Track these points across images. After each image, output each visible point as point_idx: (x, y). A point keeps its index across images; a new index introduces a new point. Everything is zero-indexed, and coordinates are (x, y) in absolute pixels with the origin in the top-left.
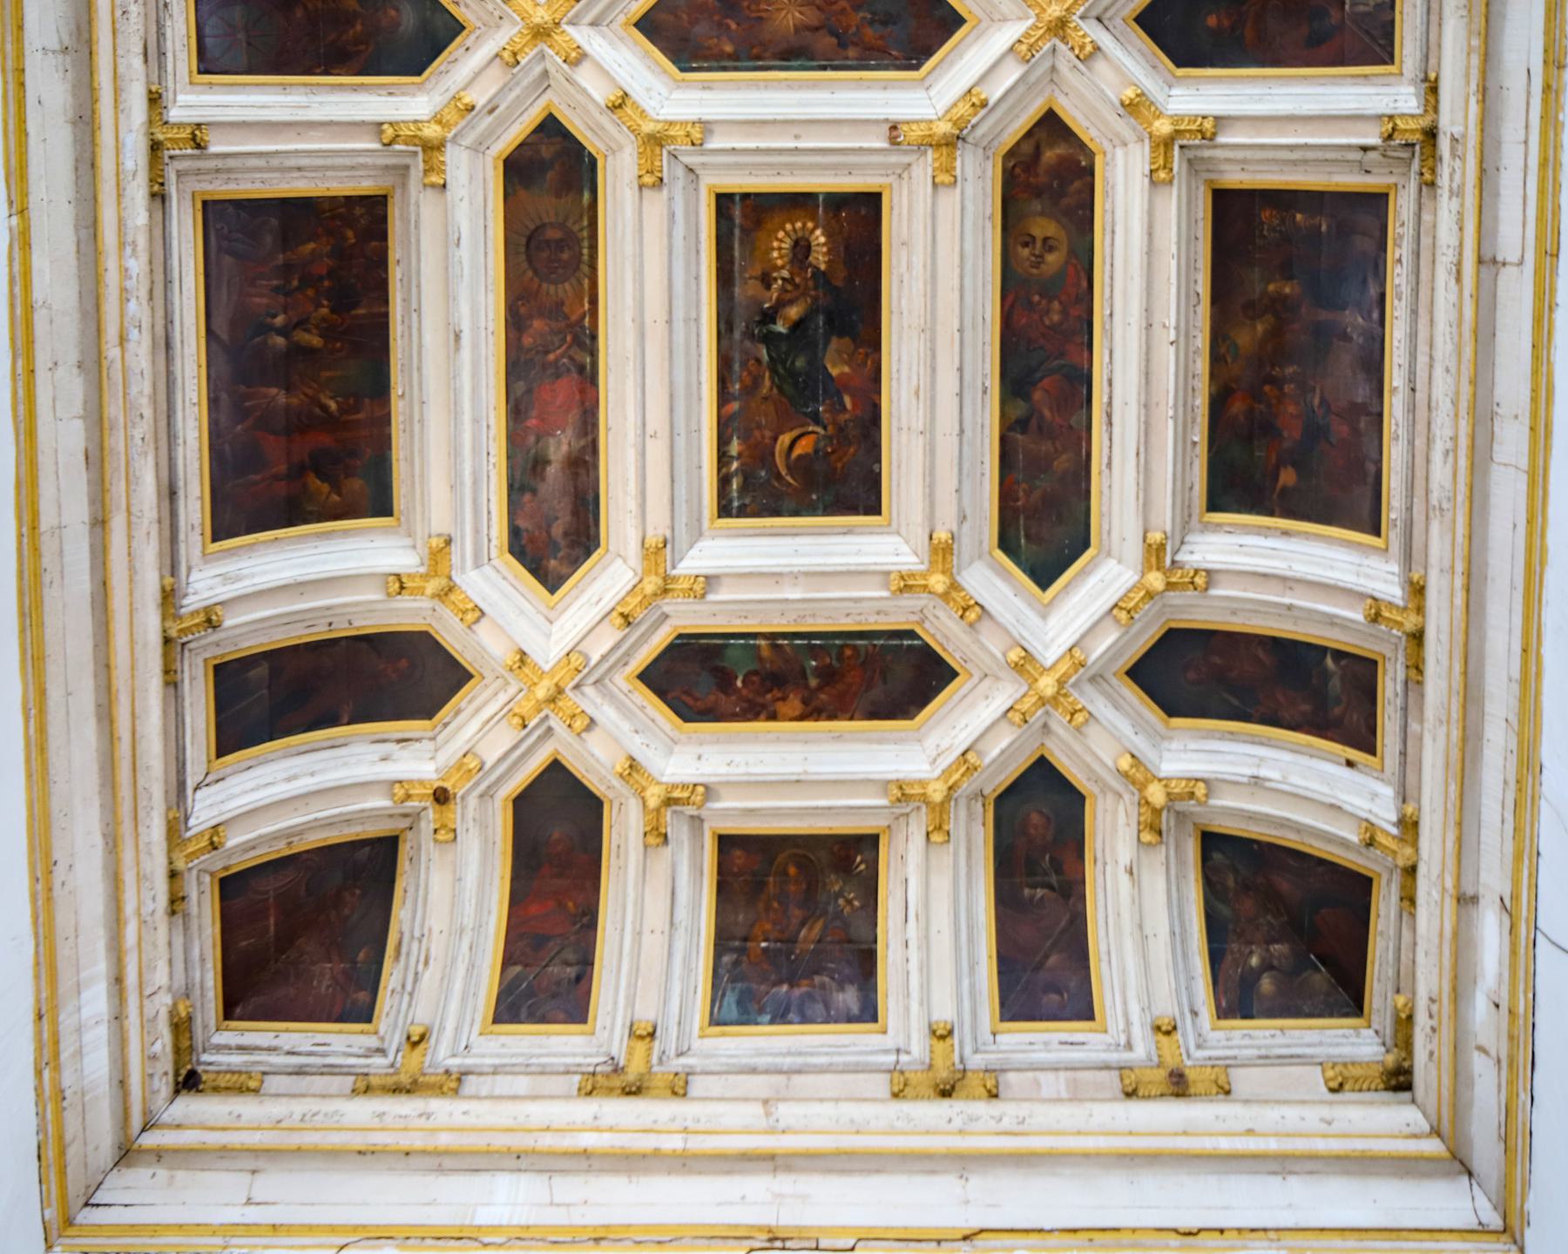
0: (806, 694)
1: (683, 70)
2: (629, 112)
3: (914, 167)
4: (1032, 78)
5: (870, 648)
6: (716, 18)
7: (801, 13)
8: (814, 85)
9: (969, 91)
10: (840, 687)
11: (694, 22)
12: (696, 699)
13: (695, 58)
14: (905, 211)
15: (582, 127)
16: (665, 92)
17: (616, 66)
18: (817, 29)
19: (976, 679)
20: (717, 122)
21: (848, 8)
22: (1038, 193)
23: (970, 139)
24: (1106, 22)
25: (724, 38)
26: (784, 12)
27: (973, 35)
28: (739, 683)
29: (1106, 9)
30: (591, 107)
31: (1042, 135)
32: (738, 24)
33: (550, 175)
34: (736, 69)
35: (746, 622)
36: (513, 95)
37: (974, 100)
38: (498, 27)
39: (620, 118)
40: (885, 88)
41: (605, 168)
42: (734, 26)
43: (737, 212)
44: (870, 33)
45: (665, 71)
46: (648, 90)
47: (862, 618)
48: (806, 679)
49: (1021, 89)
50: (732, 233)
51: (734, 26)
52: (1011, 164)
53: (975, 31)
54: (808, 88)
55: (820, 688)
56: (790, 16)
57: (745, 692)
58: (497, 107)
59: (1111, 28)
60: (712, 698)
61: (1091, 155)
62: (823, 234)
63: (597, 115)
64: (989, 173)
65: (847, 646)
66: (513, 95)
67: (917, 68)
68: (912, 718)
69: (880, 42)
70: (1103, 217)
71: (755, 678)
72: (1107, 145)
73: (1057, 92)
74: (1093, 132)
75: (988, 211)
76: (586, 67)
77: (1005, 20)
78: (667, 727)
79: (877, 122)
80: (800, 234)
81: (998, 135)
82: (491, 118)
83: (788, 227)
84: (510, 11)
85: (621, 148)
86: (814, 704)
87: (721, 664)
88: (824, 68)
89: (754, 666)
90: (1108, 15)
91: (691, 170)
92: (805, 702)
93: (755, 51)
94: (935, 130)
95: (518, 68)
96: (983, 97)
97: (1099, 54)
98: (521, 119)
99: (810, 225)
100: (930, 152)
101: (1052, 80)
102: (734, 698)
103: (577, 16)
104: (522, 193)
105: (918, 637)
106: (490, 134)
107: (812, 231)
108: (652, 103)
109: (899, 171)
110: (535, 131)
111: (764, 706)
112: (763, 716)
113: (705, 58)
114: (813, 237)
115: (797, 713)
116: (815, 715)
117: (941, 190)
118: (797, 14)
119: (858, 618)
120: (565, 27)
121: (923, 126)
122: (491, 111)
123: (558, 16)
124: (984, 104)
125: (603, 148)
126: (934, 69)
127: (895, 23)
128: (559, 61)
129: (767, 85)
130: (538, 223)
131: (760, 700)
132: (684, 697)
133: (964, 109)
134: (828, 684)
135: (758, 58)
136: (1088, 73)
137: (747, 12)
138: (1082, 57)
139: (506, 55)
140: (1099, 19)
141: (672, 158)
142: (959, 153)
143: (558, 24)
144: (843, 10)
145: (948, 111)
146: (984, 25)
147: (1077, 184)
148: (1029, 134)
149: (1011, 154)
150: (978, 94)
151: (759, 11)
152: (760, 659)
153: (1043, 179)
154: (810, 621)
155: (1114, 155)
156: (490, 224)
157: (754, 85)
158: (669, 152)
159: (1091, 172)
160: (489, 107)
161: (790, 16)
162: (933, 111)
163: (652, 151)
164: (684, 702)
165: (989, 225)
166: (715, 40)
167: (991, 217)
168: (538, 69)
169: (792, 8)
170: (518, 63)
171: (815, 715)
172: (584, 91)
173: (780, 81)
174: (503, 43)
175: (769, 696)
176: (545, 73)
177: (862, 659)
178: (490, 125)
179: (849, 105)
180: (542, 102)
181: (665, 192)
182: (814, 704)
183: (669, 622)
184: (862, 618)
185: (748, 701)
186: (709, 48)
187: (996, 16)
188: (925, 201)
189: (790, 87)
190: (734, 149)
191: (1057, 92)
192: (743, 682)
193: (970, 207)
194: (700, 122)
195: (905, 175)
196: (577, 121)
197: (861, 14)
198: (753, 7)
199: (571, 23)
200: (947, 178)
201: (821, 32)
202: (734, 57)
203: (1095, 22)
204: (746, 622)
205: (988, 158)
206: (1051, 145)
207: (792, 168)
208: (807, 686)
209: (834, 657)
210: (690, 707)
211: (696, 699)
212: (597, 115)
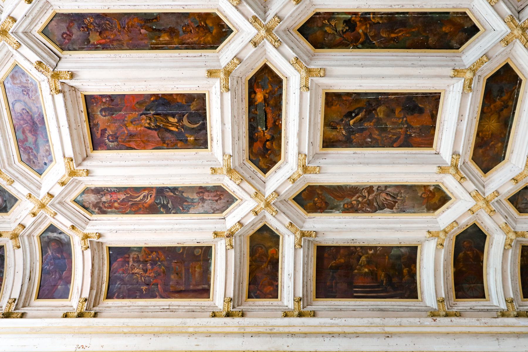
120: (486, 197)
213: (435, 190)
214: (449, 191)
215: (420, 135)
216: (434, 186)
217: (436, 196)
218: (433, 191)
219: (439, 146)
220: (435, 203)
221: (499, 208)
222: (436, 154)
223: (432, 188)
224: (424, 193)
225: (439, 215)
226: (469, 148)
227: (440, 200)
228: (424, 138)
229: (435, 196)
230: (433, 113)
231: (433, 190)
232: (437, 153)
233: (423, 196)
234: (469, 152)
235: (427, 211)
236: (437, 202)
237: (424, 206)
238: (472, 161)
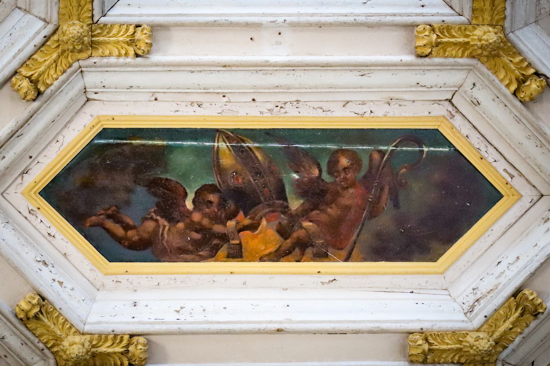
0: (284, 219)
5: (376, 156)
10: (333, 211)
12: (127, 227)
19: (525, 203)
28: (189, 204)
35: (200, 112)
47: (366, 108)
48: (285, 199)
55: (305, 213)
57: (196, 217)
60: (150, 225)
65: (343, 152)
68: (434, 260)
71: (213, 197)
78: (86, 266)
86: (298, 233)
87: (164, 176)
89: (212, 180)
92: (283, 232)
102: (181, 225)
105: (443, 141)
111: (224, 238)
112: (223, 252)
115: (272, 249)
116: (297, 251)
119: (360, 109)
131: (218, 228)
132: (110, 224)
134: (315, 207)
152: (220, 170)
154: (291, 111)
164: (108, 231)
171: (297, 251)
175: (231, 224)
177: (362, 173)
182: (298, 233)
183: (93, 109)
184: (366, 108)
185: (200, 229)
192: (194, 202)
204: (200, 112)
208: (285, 209)
209: (324, 168)
210: (119, 240)
211: (127, 227)
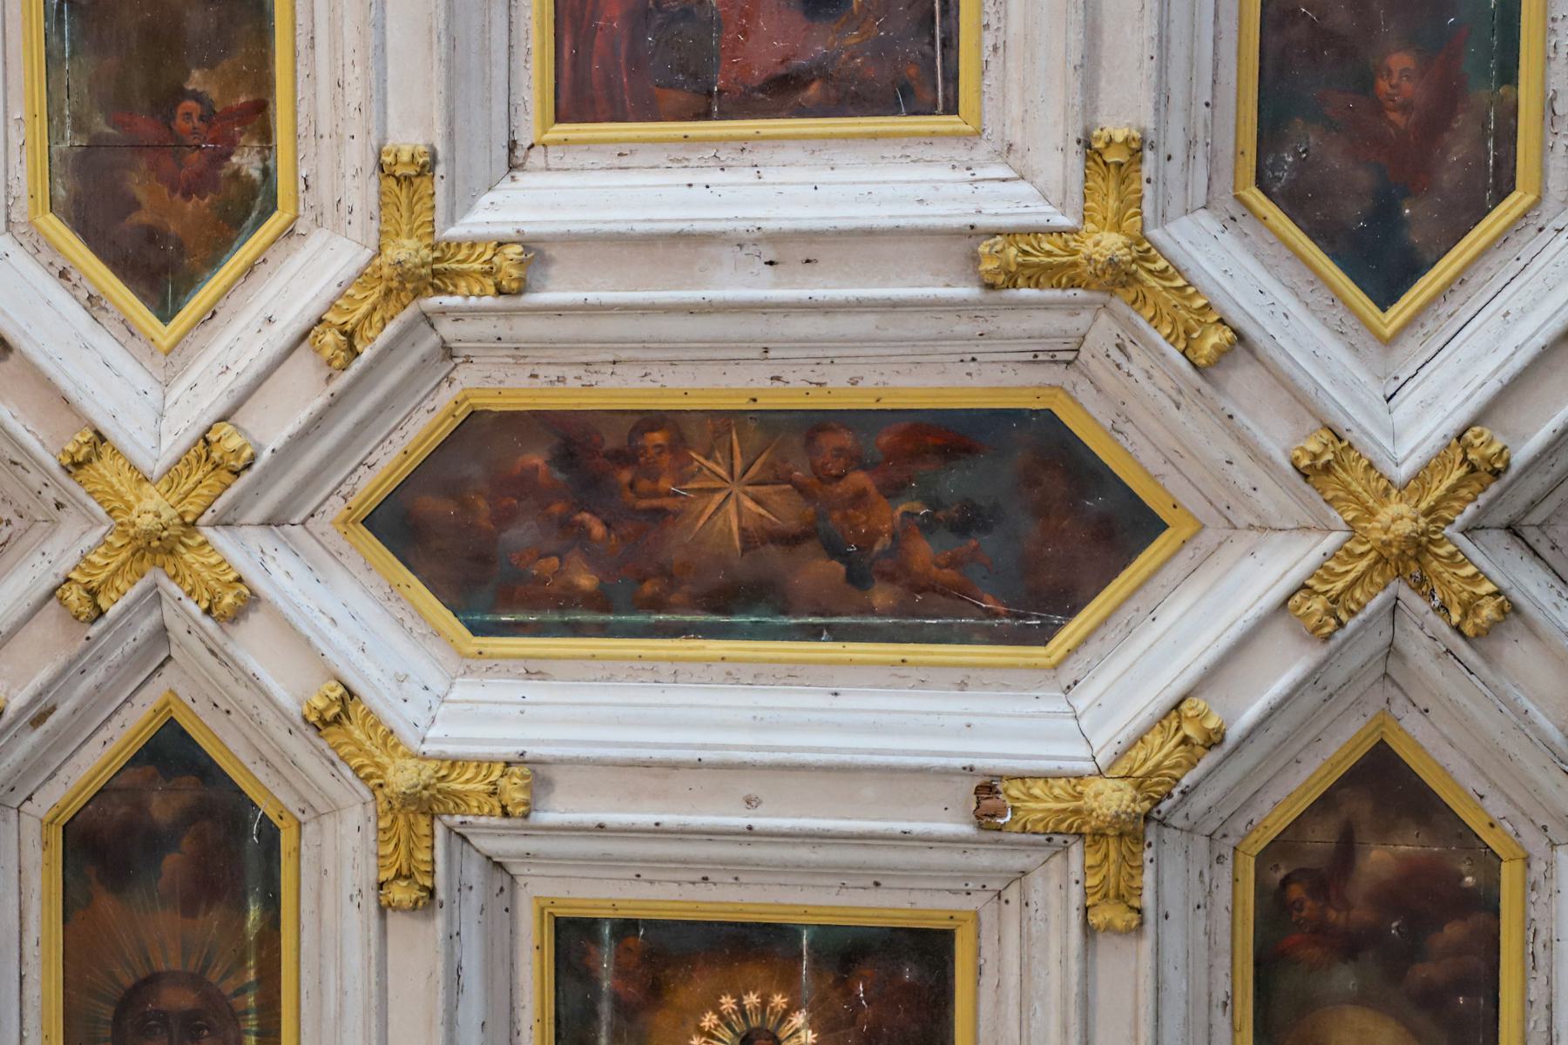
1: (477, 630)
2: (358, 734)
3: (1036, 880)
4: (1336, 676)
6: (556, 509)
7: (758, 502)
8: (791, 674)
9: (1177, 707)
11: (504, 518)
13: (507, 599)
14: (1012, 980)
15: (246, 757)
16: (438, 685)
17: (324, 623)
18: (790, 540)
20: (561, 761)
21: (873, 490)
22: (1350, 947)
23: (1176, 819)
24: (1531, 535)
25: (575, 558)
26: (719, 497)
27: (1182, 562)
29: (1533, 505)
30: (268, 716)
31: (1360, 807)
32: (608, 525)
33: (172, 862)
34: (604, 631)
36: (89, 681)
37: (1188, 729)
38: (53, 523)
39: (335, 748)
40: (963, 686)
41: (298, 850)
42: (598, 530)
43: (605, 962)
44: (924, 553)
45: (438, 633)
46: (401, 679)
49: (1310, 699)
50: (595, 1015)
51: (598, 530)
52: (1280, 875)
53: (1188, 552)
54: (776, 680)
56: (731, 507)
58: (54, 709)
59: (1543, 548)
61: (1490, 862)
62: (811, 1024)
63: (282, 735)
64: (1224, 895)
66: (89, 681)
67: (1042, 637)
69: (948, 575)
70: (1524, 1019)
72: (1533, 841)
73: (1399, 702)
74: (1495, 806)
75: (1222, 988)
76: (255, 627)
77: (1265, 528)
79: (945, 773)
80: (755, 1021)
81: (1246, 805)
82: (36, 736)
83: (728, 1003)
84: (81, 493)
85: (336, 809)
88: (813, 634)
90: (1537, 517)
91: (499, 866)
93: (649, 588)
94: (1089, 802)
95: (101, 624)
96: (1212, 724)
97: (1515, 621)
98: (104, 734)
99: (779, 1001)
100: (1076, 850)
101: (1386, 675)
103: (234, 505)
104: (106, 904)
106: (38, 767)
107: (785, 1016)
108: (412, 712)
109: (998, 886)
110: (134, 761)
113: (533, 604)
114: (785, 1031)
117: (1104, 943)
118: (749, 504)
121: (1059, 787)
122: (38, 721)
123: (192, 509)
124: (1213, 740)
125: (293, 806)
126: (1084, 641)
127: (986, 528)
128: (197, 611)
129: (678, 672)
130: (142, 973)
133: (1161, 750)
135: (656, 605)
136: (1485, 671)
137: (629, 495)
138: (1468, 628)
139: (74, 595)
140: (1513, 530)
141: (457, 841)
142: (1148, 854)
143: (191, 526)
144: (860, 497)
145: (1119, 756)
146: (1209, 537)
147: (1454, 931)
148: (1326, 803)
149: (1280, 848)
150: (1201, 717)
151: (656, 494)
153: (1361, 915)
155: (1550, 864)
156: (33, 975)
157: (648, 670)
158: (450, 829)
159: (1486, 903)
160: (34, 711)
161: (731, 507)
162: (1084, 751)
163: (410, 826)
165: (1222, 1022)
166: (555, 561)
167: (1229, 1004)
168: (146, 625)
169: (736, 490)
170: (101, 614)
172: (253, 680)
173: (709, 661)
174: (64, 566)
176: (162, 632)
178: (35, 749)
179: (876, 729)
180: (152, 696)
181: (440, 921)
186: (541, 580)
187: (1243, 518)
188: (1063, 962)
189: (731, 678)
190: (601, 827)
191: (1399, 702)
193: (1176, 983)
194: (522, 760)
195: (1012, 894)
196: (235, 743)
197: (902, 508)
198: (644, 485)
199: (222, 522)
200: (1118, 916)
201: (809, 547)
202: (599, 601)
203: (1503, 539)
205: (1220, 859)
206: (1384, 834)
207: (737, 871)
212: (282, 735)
213: (233, 189)
214: (227, 292)
215: (647, 13)
216: (267, 173)
217: (190, 206)
218: (225, 172)
219: (568, 161)
220: (135, 205)
221: (116, 656)
222: (512, 146)
223: (246, 161)
224: (208, 116)
225: (38, 245)
226: (554, 373)
227: (152, 235)
228: (623, 49)
229: (187, 195)
230: (806, 85)
231: (236, 175)
232: (519, 153)
233: (189, 105)
234: (525, 382)
235: (63, 158)
236: (143, 217)
237: (100, 125)
238: (462, 414)
